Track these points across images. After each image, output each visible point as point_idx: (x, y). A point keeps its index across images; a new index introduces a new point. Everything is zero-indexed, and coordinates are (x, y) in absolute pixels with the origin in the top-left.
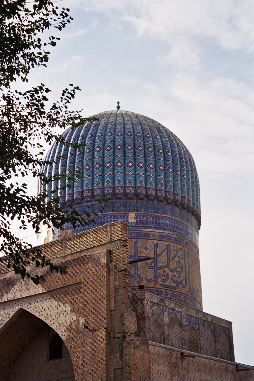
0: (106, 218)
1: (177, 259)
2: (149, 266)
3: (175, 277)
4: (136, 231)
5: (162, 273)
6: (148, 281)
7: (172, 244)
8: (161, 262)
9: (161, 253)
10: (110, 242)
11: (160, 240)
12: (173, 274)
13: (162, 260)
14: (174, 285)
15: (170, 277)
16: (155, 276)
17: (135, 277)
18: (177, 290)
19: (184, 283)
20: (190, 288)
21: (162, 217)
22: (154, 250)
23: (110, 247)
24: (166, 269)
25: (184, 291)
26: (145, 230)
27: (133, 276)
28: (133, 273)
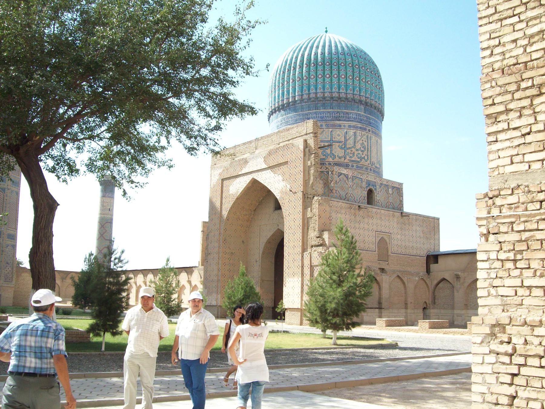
6: (340, 158)
9: (350, 138)
10: (306, 134)
13: (350, 143)
14: (359, 160)
15: (355, 154)
19: (366, 158)
20: (371, 161)
21: (351, 113)
23: (305, 137)
24: (353, 149)
25: (366, 164)
26: (338, 122)
28: (329, 152)
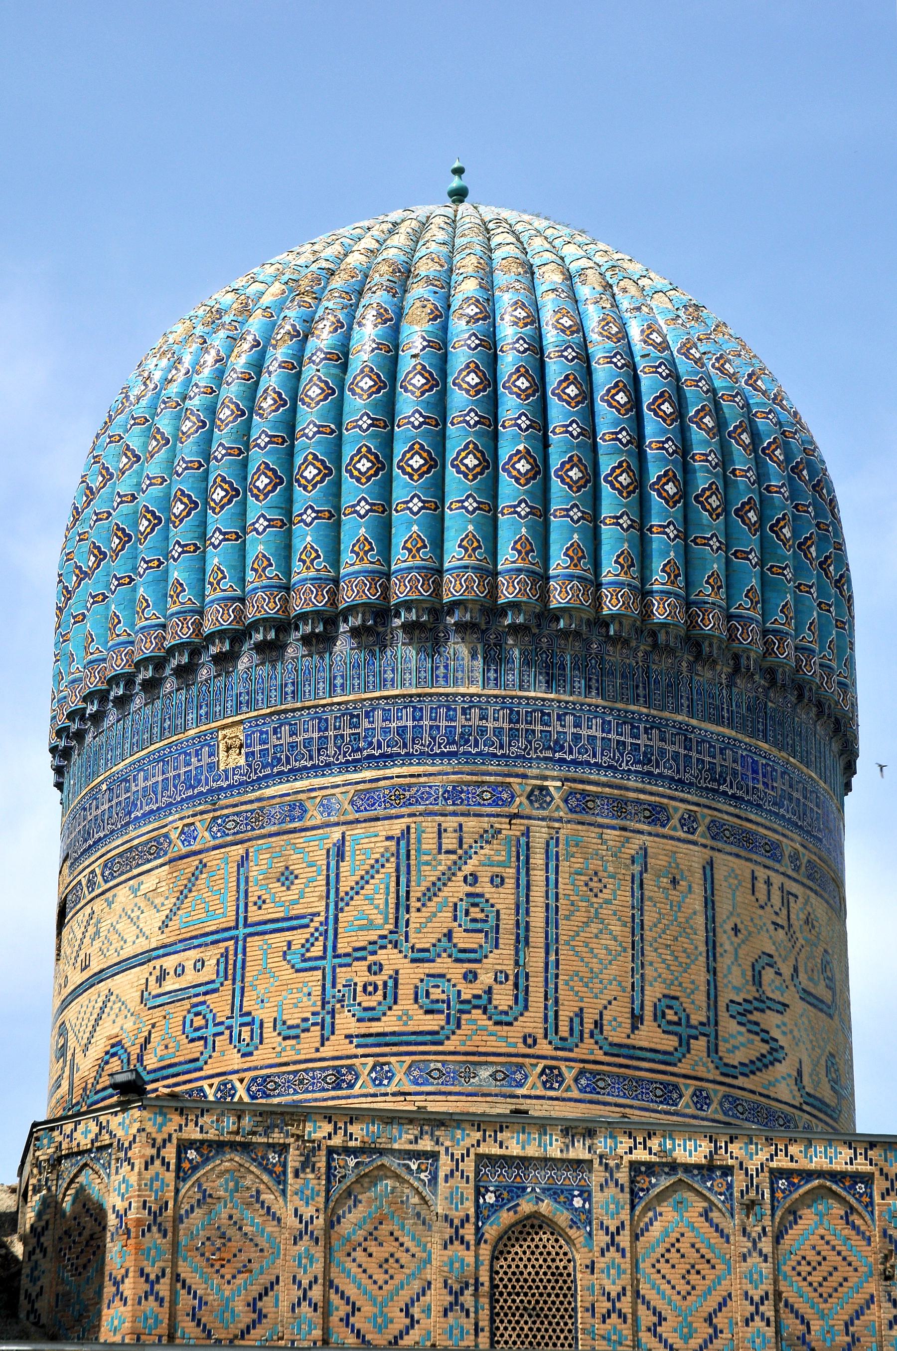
0: (570, 719)
1: (457, 889)
2: (296, 959)
3: (438, 981)
4: (244, 808)
7: (430, 825)
8: (361, 928)
11: (357, 821)
12: (427, 968)
14: (433, 1023)
15: (405, 992)
16: (324, 1003)
17: (230, 1028)
18: (449, 1046)
19: (503, 998)
20: (551, 1020)
22: (328, 876)
24: (389, 958)
26: (284, 788)
27: (222, 1023)
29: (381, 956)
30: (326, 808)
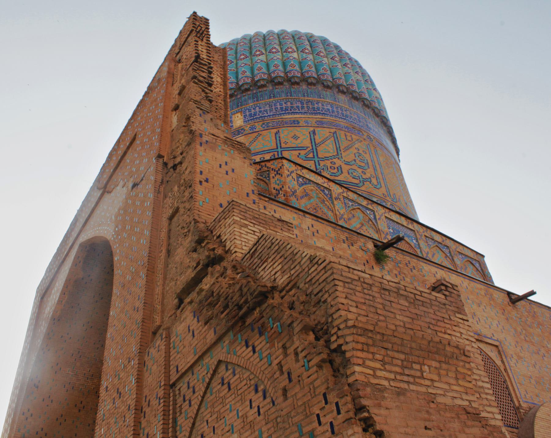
5: (329, 165)
7: (342, 133)
9: (323, 142)
26: (290, 116)
29: (334, 160)
30: (307, 122)
